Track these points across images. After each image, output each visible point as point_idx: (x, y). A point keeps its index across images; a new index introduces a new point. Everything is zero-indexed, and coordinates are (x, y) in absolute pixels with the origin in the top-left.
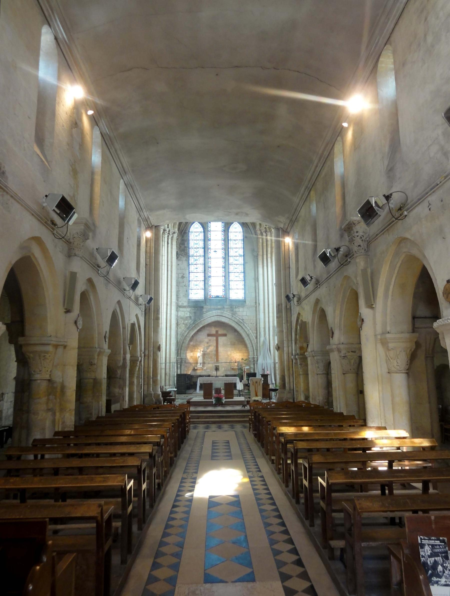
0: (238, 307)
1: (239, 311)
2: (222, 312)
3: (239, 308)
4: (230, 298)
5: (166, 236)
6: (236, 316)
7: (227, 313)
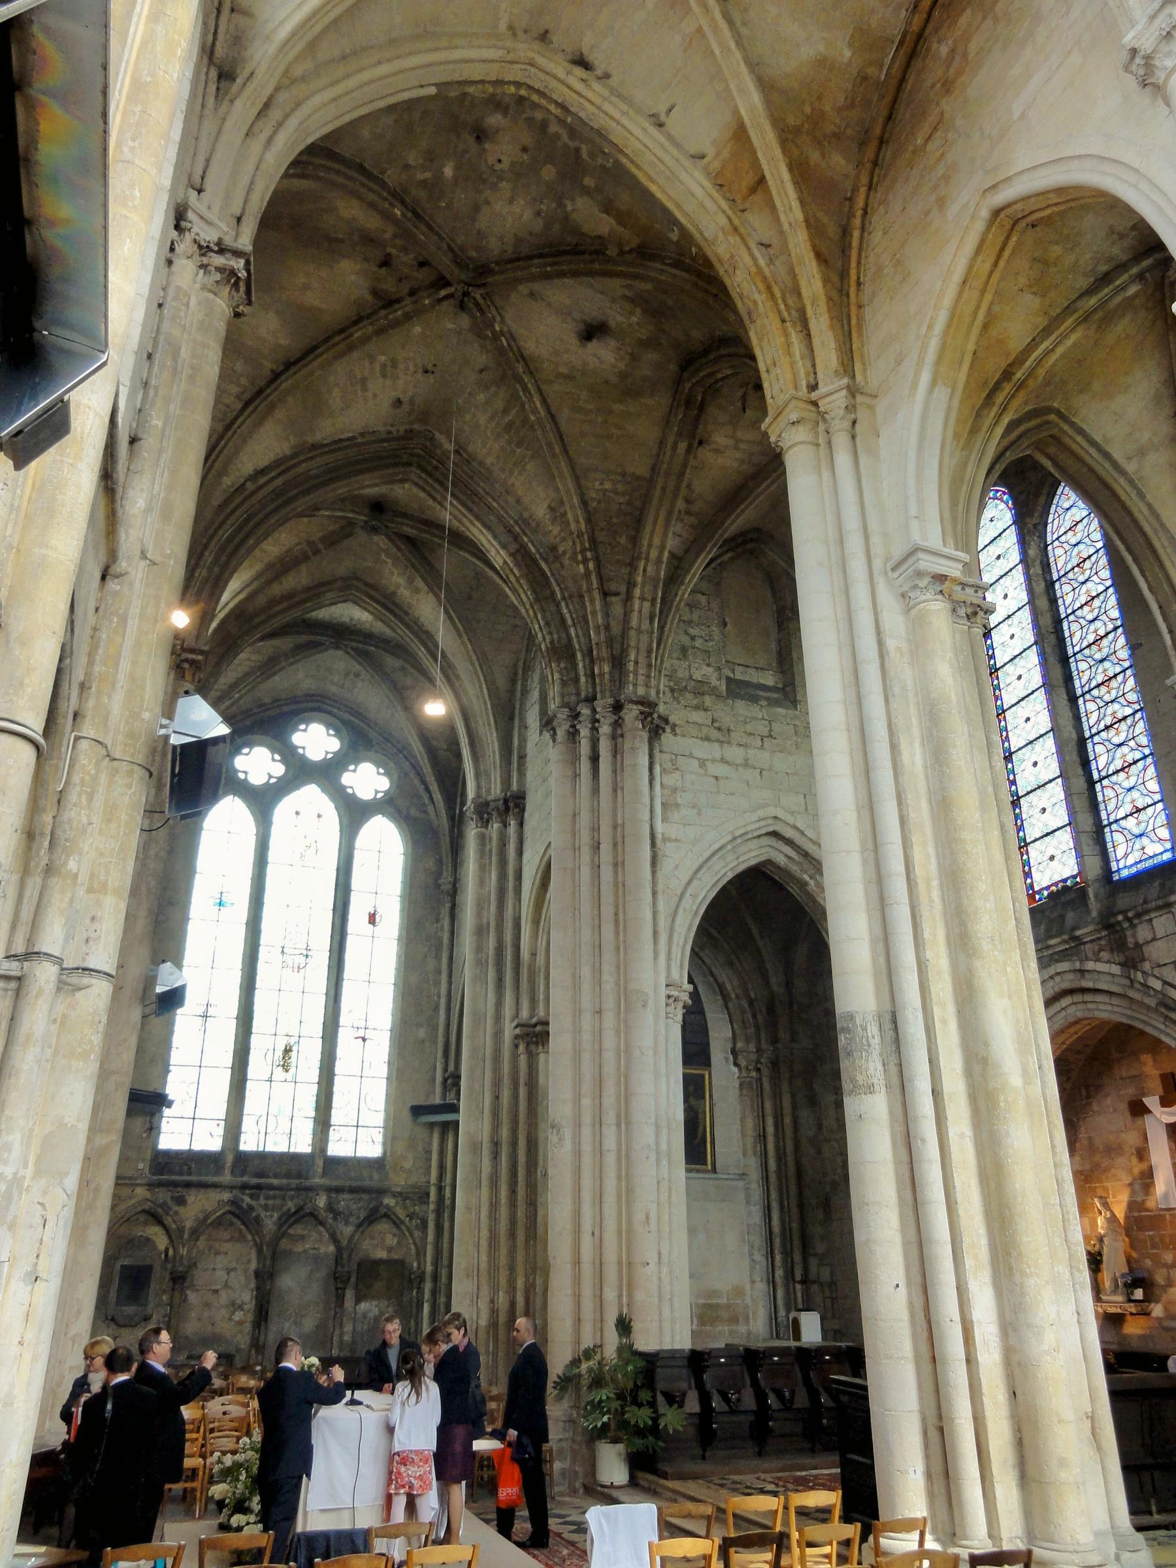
0: (1139, 915)
1: (1154, 939)
2: (1077, 965)
3: (1150, 920)
4: (1116, 877)
5: (584, 732)
6: (1144, 973)
7: (1101, 967)
